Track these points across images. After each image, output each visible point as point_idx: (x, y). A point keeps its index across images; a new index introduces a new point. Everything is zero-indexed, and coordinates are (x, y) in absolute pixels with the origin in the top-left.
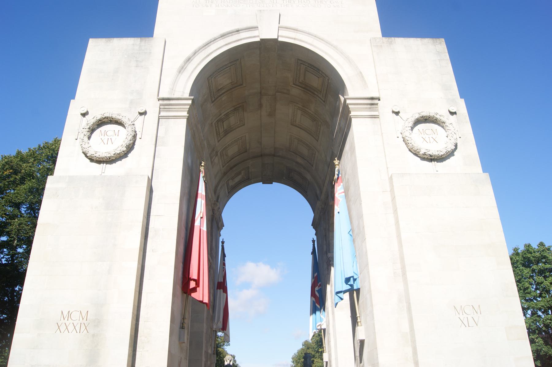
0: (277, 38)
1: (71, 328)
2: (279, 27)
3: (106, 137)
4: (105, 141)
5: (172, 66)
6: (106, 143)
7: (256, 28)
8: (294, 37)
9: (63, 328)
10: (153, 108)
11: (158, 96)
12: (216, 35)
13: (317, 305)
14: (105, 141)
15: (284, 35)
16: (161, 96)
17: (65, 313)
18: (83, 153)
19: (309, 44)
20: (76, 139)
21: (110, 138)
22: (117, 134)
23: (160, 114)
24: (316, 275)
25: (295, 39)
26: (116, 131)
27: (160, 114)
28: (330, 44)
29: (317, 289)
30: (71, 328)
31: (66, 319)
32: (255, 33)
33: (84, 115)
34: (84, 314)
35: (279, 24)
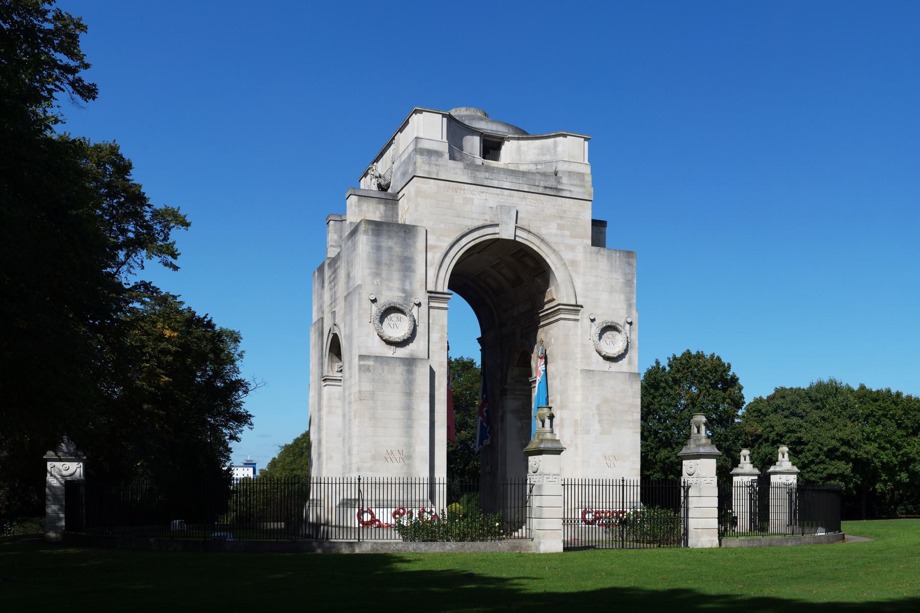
0: (513, 239)
1: (394, 460)
2: (516, 227)
3: (392, 323)
4: (392, 326)
5: (435, 257)
6: (392, 327)
7: (497, 225)
8: (526, 238)
9: (389, 460)
10: (422, 297)
11: (426, 289)
12: (466, 230)
13: (484, 424)
14: (392, 326)
15: (520, 235)
16: (429, 289)
17: (389, 452)
18: (378, 335)
19: (537, 246)
20: (370, 322)
21: (395, 323)
22: (399, 320)
23: (429, 304)
24: (485, 396)
25: (526, 240)
26: (399, 318)
27: (429, 304)
28: (551, 248)
29: (485, 409)
30: (394, 460)
31: (390, 455)
32: (496, 230)
33: (374, 301)
34: (401, 452)
35: (516, 223)
